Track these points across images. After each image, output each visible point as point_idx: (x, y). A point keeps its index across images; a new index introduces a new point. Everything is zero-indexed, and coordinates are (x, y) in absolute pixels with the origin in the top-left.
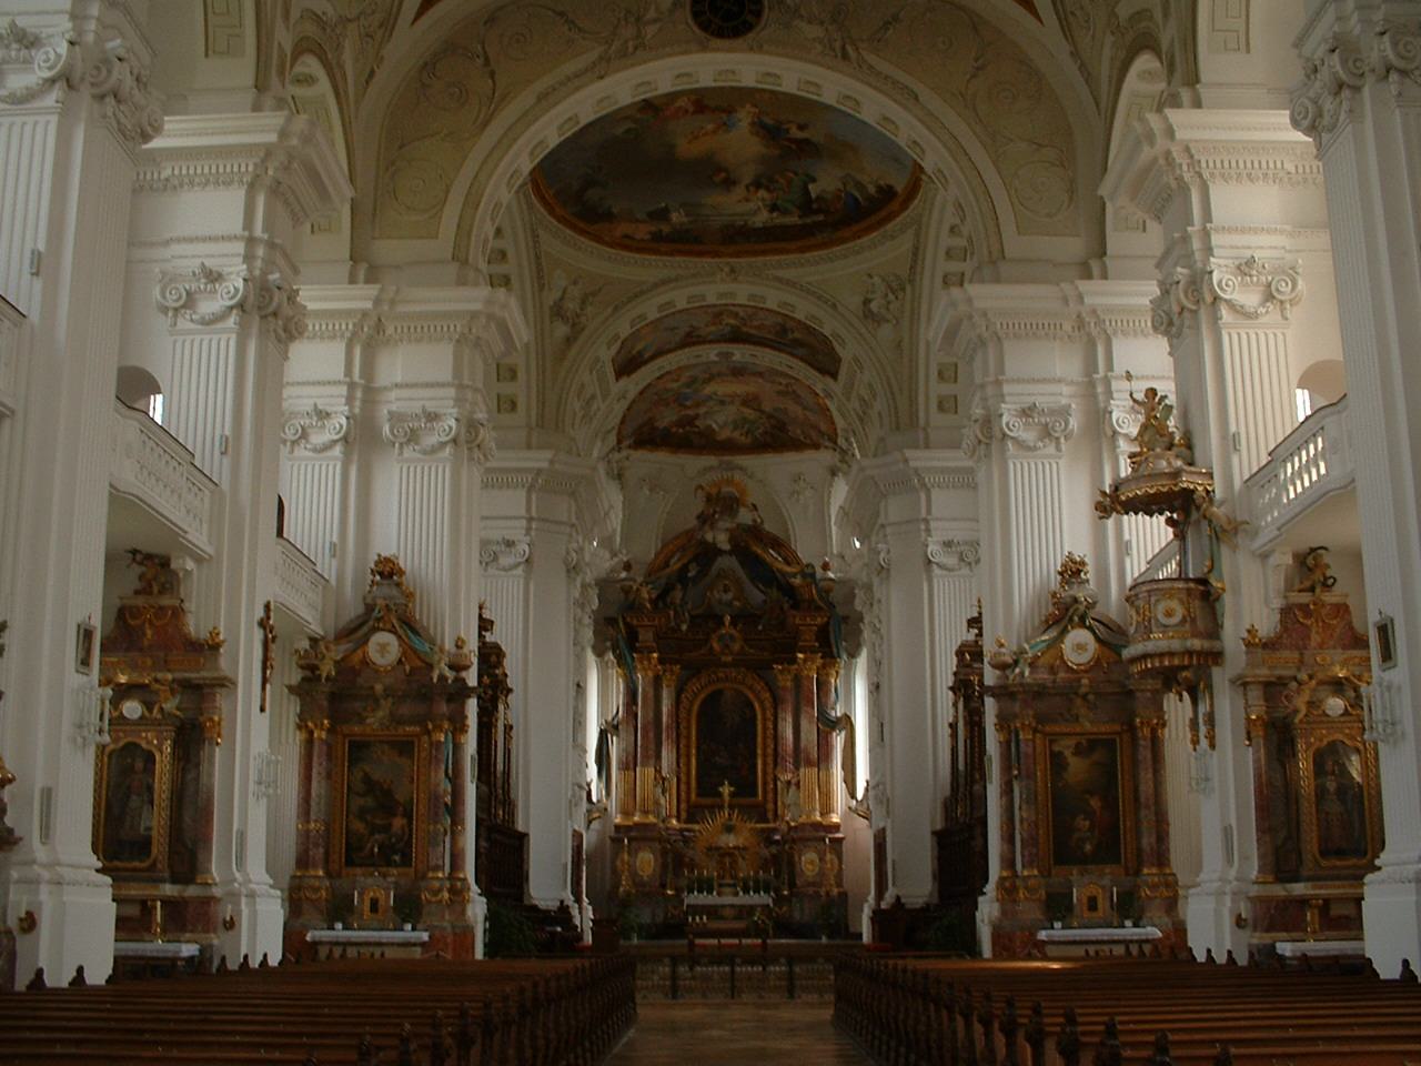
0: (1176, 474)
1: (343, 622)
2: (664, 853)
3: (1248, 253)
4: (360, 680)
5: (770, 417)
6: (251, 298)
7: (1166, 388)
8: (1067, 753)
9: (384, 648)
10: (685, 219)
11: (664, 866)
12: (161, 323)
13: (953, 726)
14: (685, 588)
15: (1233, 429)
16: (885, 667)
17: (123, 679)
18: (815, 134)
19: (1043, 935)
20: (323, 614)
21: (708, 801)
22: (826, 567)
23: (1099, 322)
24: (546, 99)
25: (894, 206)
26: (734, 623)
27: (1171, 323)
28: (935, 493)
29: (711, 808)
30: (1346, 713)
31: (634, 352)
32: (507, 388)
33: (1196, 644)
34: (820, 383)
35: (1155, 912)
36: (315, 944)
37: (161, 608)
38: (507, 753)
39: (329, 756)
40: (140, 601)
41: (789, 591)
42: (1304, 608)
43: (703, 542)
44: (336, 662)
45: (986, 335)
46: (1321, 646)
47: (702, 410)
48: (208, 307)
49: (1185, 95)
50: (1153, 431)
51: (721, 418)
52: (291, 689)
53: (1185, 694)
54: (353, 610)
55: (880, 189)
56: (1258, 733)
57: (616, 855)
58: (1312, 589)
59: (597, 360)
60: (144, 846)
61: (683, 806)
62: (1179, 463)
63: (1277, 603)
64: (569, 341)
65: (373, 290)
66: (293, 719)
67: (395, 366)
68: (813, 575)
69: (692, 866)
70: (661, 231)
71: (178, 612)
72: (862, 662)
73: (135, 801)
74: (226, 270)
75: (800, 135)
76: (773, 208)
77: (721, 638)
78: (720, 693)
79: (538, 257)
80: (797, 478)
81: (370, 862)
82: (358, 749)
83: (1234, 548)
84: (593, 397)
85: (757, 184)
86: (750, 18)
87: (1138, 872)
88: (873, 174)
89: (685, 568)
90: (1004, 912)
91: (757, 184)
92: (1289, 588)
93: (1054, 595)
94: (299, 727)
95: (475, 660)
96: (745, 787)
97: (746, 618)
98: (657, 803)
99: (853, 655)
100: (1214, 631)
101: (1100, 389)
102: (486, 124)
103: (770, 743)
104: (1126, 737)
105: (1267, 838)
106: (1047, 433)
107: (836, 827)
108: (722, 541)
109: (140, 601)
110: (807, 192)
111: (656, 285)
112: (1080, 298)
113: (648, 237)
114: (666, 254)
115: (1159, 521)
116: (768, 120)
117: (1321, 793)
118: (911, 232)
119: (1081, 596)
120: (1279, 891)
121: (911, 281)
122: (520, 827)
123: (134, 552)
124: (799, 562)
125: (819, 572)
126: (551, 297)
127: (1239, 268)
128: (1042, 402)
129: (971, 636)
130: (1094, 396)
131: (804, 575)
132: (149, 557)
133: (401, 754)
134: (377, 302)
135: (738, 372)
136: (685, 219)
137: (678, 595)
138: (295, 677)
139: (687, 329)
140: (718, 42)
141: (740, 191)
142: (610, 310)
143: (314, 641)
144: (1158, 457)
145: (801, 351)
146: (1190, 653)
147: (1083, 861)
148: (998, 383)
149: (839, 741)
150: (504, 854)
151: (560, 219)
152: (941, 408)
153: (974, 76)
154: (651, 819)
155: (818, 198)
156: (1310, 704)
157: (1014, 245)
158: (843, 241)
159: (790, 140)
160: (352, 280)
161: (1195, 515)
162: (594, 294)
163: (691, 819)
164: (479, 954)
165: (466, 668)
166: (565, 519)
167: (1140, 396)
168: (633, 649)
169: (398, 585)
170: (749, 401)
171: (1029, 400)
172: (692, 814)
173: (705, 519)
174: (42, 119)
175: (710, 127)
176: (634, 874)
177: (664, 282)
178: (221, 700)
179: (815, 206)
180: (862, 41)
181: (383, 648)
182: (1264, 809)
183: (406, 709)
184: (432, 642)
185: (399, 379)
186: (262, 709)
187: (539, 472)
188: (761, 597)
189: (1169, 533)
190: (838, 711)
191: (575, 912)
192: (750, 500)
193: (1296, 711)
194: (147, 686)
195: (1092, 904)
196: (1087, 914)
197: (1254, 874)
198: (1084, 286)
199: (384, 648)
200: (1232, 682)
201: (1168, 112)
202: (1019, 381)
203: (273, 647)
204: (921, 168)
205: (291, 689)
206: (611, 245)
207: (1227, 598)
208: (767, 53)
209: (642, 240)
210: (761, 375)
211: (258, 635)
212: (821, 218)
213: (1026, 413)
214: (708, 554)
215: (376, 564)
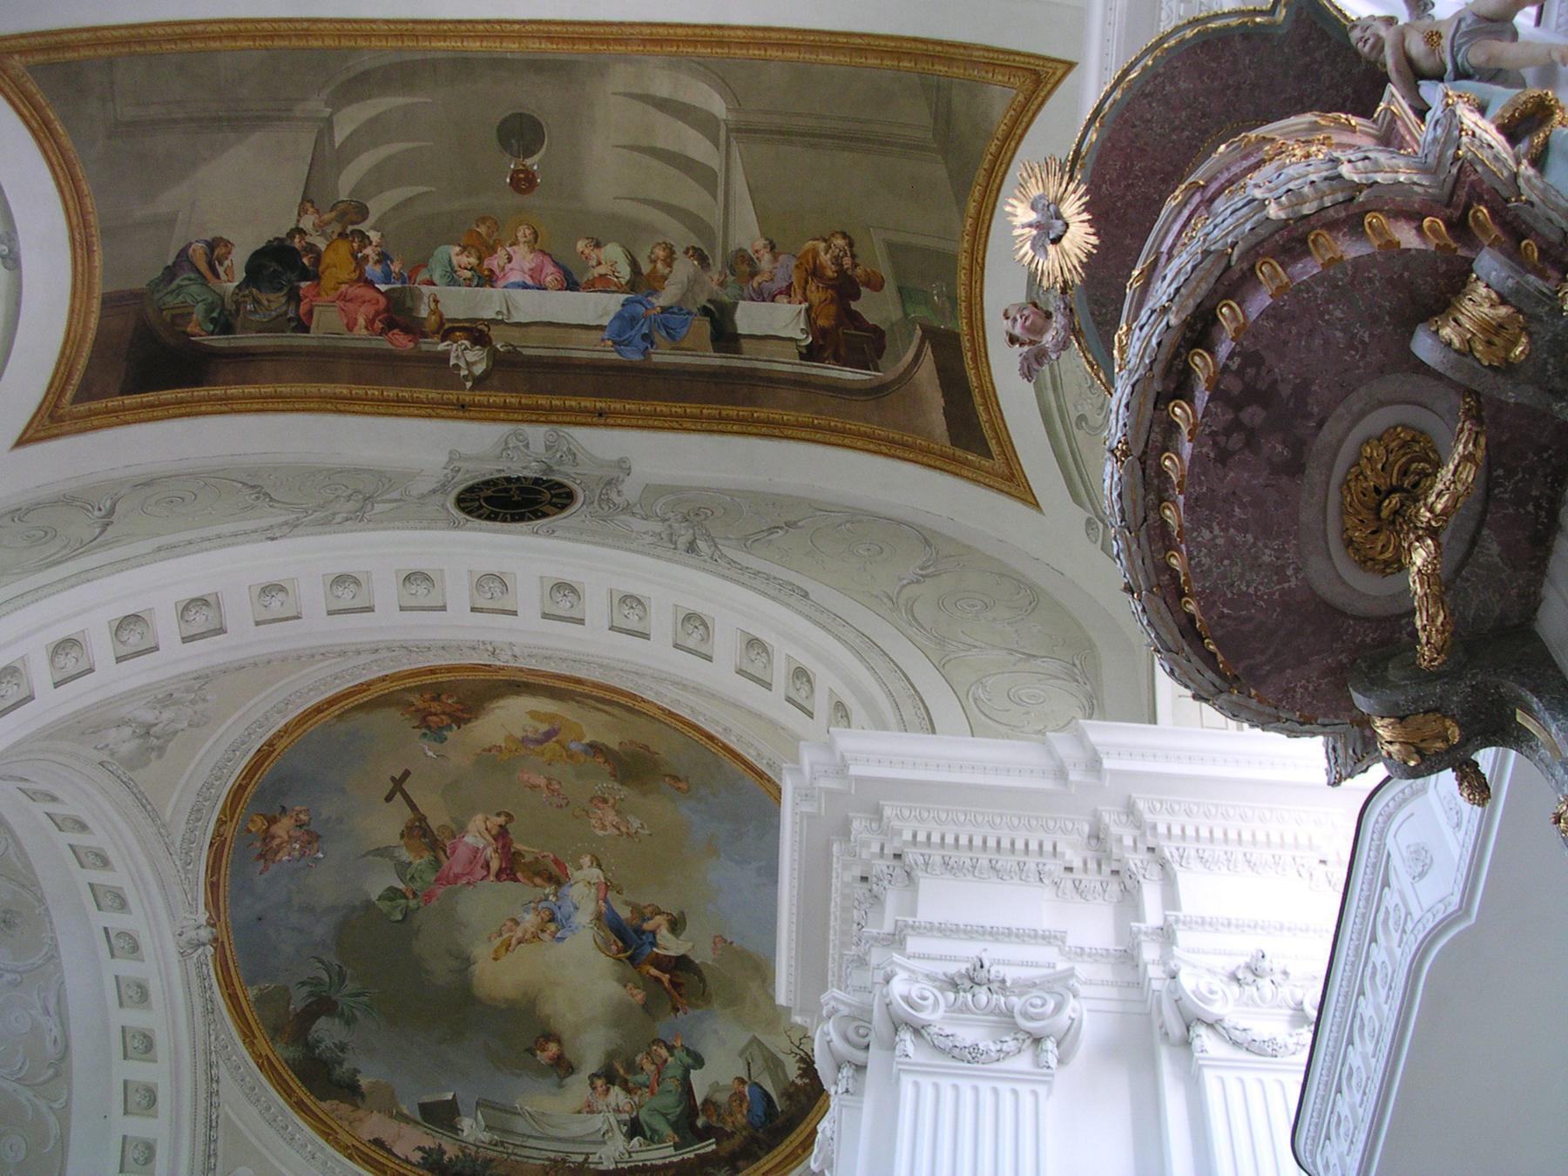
10: (485, 1136)
76: (635, 1128)
79: (211, 1126)
85: (609, 1076)
110: (688, 1090)
113: (416, 1157)
116: (624, 913)
136: (485, 1136)
140: (478, 522)
141: (578, 1087)
151: (265, 1064)
155: (706, 1101)
159: (661, 963)
175: (530, 920)
179: (700, 1123)
198: (1100, 733)
206: (352, 1153)
209: (407, 1161)
212: (709, 1146)
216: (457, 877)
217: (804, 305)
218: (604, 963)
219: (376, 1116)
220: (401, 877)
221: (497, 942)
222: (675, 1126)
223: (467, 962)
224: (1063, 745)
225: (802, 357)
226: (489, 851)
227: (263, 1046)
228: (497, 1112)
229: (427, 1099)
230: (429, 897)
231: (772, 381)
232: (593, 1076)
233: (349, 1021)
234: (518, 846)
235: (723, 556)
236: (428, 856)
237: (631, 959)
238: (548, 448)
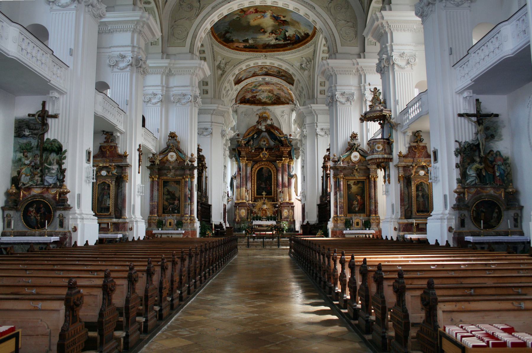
0: (382, 110)
1: (162, 149)
2: (248, 210)
3: (402, 51)
4: (166, 165)
5: (276, 95)
6: (134, 63)
7: (380, 88)
8: (352, 184)
9: (172, 156)
11: (248, 213)
12: (109, 69)
13: (323, 177)
14: (253, 141)
15: (397, 99)
16: (305, 162)
17: (101, 165)
18: (287, 19)
19: (345, 232)
20: (156, 147)
21: (259, 196)
22: (290, 135)
23: (363, 70)
24: (214, 9)
25: (309, 39)
26: (266, 150)
27: (381, 70)
28: (319, 116)
29: (260, 198)
30: (425, 175)
32: (205, 88)
33: (386, 156)
34: (289, 86)
35: (374, 226)
36: (155, 234)
37: (111, 146)
38: (206, 184)
39: (158, 185)
40: (105, 144)
41: (281, 142)
42: (414, 147)
43: (258, 129)
44: (160, 160)
45: (332, 73)
46: (419, 157)
47: (258, 94)
48: (122, 65)
49: (387, 7)
50: (376, 99)
51: (263, 96)
52: (147, 167)
53: (383, 169)
54: (164, 146)
55: (305, 34)
56: (402, 180)
57: (235, 210)
58: (417, 142)
59: (229, 80)
60: (108, 209)
61: (253, 198)
62: (382, 108)
63: (408, 146)
64: (222, 75)
65: (168, 61)
66: (148, 175)
67: (175, 81)
68: (287, 137)
69: (255, 213)
71: (116, 147)
72: (299, 160)
73: (105, 197)
74: (127, 55)
75: (283, 19)
76: (276, 39)
77: (263, 154)
78: (262, 168)
79: (213, 52)
80: (283, 112)
81: (169, 213)
82: (166, 183)
83: (397, 131)
84: (229, 90)
85: (272, 33)
87: (369, 216)
88: (303, 30)
89: (253, 135)
90: (334, 226)
91: (272, 33)
92: (411, 141)
93: (349, 143)
94: (150, 178)
95: (196, 159)
96: (269, 193)
97: (269, 149)
98: (246, 197)
99: (297, 158)
100: (391, 153)
101: (362, 88)
102: (198, 15)
103: (276, 181)
104: (367, 181)
105: (403, 207)
106: (348, 100)
107: (293, 203)
108: (263, 128)
109: (105, 144)
110: (285, 35)
111: (245, 60)
112: (358, 64)
115: (377, 123)
117: (417, 196)
118: (313, 45)
119: (356, 143)
120: (406, 221)
121: (313, 59)
122: (210, 203)
123: (104, 131)
124: (283, 134)
125: (289, 137)
126: (217, 63)
127: (400, 55)
128: (347, 91)
129: (327, 154)
130: (361, 90)
131: (285, 138)
132: (107, 132)
133: (177, 184)
134: (169, 64)
135: (267, 83)
137: (251, 142)
138: (149, 164)
141: (267, 34)
143: (154, 155)
144: (377, 106)
145: (284, 78)
146: (384, 158)
147: (355, 212)
148: (335, 86)
149: (293, 181)
150: (205, 211)
151: (219, 42)
152: (321, 93)
153: (330, 2)
154: (244, 201)
156: (415, 172)
157: (340, 49)
158: (295, 48)
160: (162, 58)
161: (386, 122)
162: (228, 62)
163: (255, 201)
164: (198, 236)
165: (194, 162)
166: (221, 122)
167: (373, 90)
168: (240, 157)
169: (176, 140)
170: (270, 91)
171: (343, 91)
172: (255, 200)
173: (258, 122)
174: (72, 12)
175: (259, 17)
176: (240, 215)
177: (247, 59)
178: (128, 170)
181: (172, 156)
182: (402, 200)
183: (178, 172)
184: (185, 155)
185: (175, 85)
186: (139, 173)
187: (214, 110)
188: (274, 143)
189: (379, 127)
190: (293, 173)
191: (224, 225)
192: (271, 118)
193: (412, 174)
194: (108, 167)
195: (358, 224)
196: (356, 226)
197: (399, 217)
198: (359, 60)
199: (172, 156)
200: (395, 166)
201: (382, 12)
202: (340, 86)
203: (141, 156)
204: (316, 28)
205: (147, 167)
206: (233, 49)
207: (394, 144)
210: (273, 84)
211: (137, 153)
212: (289, 42)
213: (343, 94)
214: (259, 132)
215: (170, 134)
218: (272, 20)
222: (283, 39)
224: (354, 61)
227: (219, 40)
233: (231, 33)
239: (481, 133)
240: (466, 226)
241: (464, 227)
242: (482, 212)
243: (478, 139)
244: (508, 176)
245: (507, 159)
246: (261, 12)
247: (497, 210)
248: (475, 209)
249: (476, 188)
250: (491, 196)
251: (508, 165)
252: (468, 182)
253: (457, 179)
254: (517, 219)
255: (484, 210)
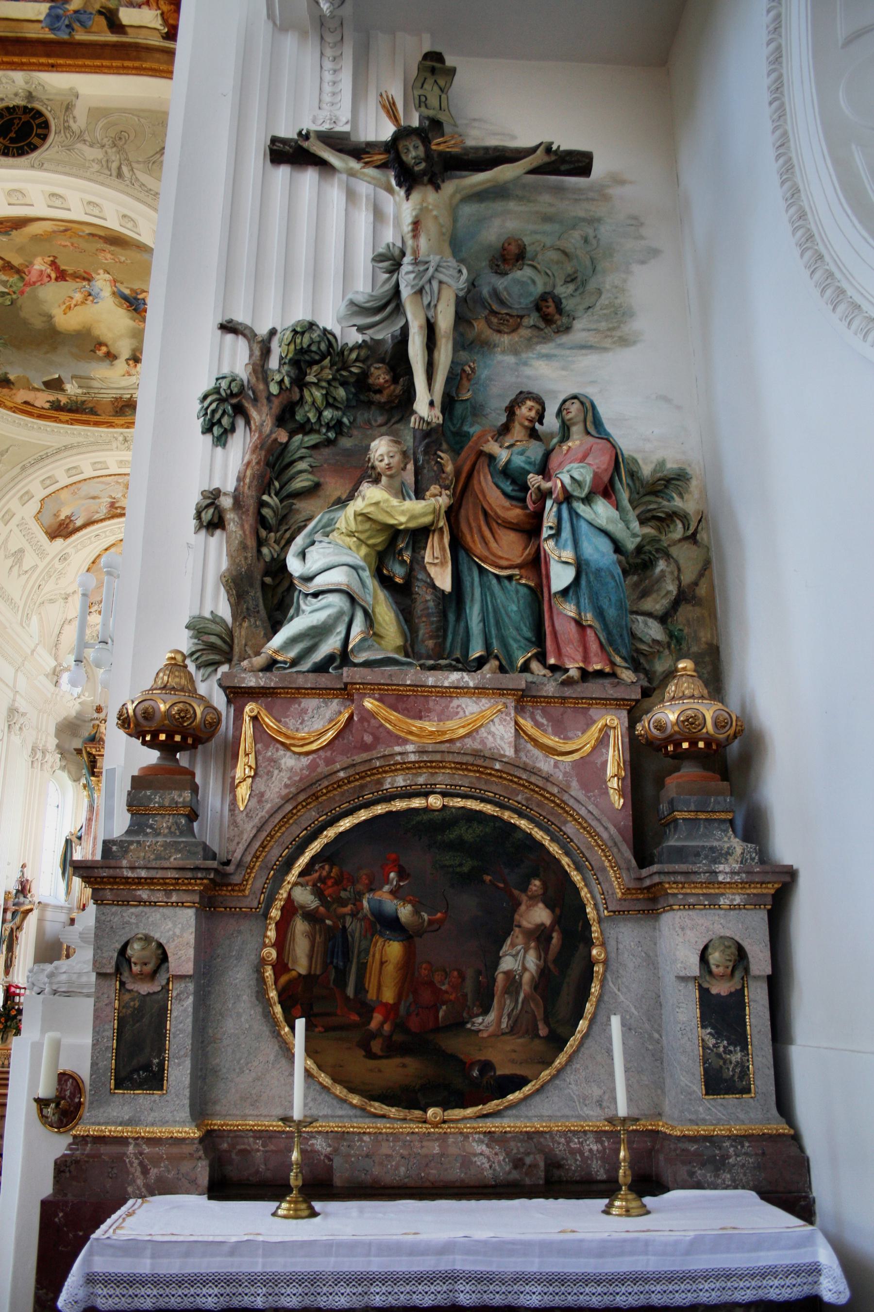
10: (80, 391)
31: (62, 517)
70: (59, 401)
86: (36, 141)
111: (59, 451)
113: (47, 405)
114: (67, 422)
116: (127, 292)
136: (80, 391)
139: (110, 500)
142: (17, 469)
175: (78, 297)
177: (66, 448)
180: (138, 162)
206: (15, 409)
208: (46, 170)
216: (34, 283)
217: (159, 12)
219: (22, 392)
220: (6, 287)
221: (64, 307)
223: (50, 317)
225: (164, 38)
226: (49, 271)
228: (81, 379)
229: (45, 379)
230: (22, 293)
231: (149, 49)
232: (127, 360)
234: (63, 267)
235: (137, 180)
236: (16, 277)
237: (135, 310)
238: (27, 83)
239: (423, 242)
240: (179, 1074)
241: (154, 1080)
242: (390, 925)
243: (396, 292)
244: (686, 612)
245: (672, 481)
246: (76, 276)
247: (540, 915)
248: (304, 897)
249: (346, 692)
250: (478, 763)
251: (678, 531)
252: (278, 640)
253: (198, 628)
254: (738, 1000)
255: (405, 912)
